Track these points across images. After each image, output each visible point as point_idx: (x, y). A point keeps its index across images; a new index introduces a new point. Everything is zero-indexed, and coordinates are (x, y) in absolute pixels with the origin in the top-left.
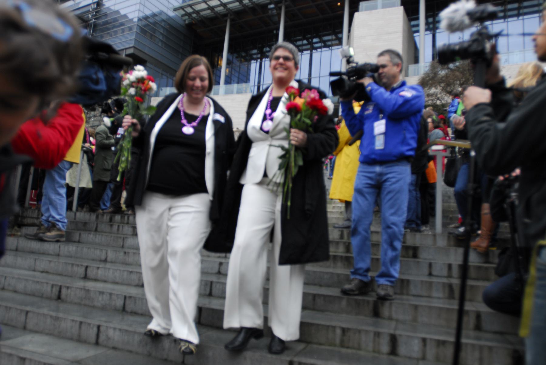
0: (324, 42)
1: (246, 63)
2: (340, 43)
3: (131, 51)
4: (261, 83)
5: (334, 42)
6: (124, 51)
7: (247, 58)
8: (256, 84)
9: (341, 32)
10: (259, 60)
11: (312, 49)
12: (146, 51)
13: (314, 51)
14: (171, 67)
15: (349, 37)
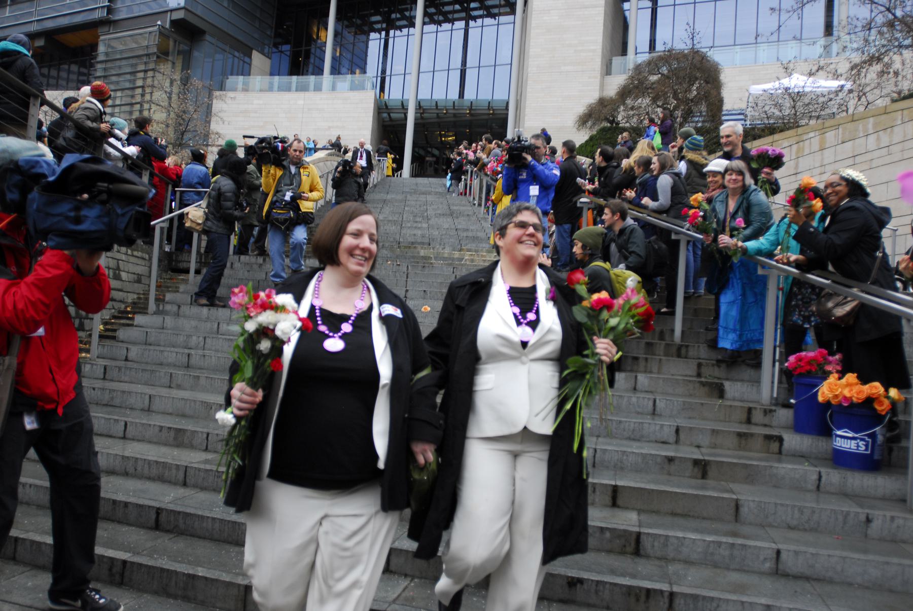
1: (363, 37)
2: (513, 12)
4: (388, 72)
5: (502, 10)
7: (366, 28)
10: (383, 33)
11: (469, 18)
12: (199, 11)
13: (472, 23)
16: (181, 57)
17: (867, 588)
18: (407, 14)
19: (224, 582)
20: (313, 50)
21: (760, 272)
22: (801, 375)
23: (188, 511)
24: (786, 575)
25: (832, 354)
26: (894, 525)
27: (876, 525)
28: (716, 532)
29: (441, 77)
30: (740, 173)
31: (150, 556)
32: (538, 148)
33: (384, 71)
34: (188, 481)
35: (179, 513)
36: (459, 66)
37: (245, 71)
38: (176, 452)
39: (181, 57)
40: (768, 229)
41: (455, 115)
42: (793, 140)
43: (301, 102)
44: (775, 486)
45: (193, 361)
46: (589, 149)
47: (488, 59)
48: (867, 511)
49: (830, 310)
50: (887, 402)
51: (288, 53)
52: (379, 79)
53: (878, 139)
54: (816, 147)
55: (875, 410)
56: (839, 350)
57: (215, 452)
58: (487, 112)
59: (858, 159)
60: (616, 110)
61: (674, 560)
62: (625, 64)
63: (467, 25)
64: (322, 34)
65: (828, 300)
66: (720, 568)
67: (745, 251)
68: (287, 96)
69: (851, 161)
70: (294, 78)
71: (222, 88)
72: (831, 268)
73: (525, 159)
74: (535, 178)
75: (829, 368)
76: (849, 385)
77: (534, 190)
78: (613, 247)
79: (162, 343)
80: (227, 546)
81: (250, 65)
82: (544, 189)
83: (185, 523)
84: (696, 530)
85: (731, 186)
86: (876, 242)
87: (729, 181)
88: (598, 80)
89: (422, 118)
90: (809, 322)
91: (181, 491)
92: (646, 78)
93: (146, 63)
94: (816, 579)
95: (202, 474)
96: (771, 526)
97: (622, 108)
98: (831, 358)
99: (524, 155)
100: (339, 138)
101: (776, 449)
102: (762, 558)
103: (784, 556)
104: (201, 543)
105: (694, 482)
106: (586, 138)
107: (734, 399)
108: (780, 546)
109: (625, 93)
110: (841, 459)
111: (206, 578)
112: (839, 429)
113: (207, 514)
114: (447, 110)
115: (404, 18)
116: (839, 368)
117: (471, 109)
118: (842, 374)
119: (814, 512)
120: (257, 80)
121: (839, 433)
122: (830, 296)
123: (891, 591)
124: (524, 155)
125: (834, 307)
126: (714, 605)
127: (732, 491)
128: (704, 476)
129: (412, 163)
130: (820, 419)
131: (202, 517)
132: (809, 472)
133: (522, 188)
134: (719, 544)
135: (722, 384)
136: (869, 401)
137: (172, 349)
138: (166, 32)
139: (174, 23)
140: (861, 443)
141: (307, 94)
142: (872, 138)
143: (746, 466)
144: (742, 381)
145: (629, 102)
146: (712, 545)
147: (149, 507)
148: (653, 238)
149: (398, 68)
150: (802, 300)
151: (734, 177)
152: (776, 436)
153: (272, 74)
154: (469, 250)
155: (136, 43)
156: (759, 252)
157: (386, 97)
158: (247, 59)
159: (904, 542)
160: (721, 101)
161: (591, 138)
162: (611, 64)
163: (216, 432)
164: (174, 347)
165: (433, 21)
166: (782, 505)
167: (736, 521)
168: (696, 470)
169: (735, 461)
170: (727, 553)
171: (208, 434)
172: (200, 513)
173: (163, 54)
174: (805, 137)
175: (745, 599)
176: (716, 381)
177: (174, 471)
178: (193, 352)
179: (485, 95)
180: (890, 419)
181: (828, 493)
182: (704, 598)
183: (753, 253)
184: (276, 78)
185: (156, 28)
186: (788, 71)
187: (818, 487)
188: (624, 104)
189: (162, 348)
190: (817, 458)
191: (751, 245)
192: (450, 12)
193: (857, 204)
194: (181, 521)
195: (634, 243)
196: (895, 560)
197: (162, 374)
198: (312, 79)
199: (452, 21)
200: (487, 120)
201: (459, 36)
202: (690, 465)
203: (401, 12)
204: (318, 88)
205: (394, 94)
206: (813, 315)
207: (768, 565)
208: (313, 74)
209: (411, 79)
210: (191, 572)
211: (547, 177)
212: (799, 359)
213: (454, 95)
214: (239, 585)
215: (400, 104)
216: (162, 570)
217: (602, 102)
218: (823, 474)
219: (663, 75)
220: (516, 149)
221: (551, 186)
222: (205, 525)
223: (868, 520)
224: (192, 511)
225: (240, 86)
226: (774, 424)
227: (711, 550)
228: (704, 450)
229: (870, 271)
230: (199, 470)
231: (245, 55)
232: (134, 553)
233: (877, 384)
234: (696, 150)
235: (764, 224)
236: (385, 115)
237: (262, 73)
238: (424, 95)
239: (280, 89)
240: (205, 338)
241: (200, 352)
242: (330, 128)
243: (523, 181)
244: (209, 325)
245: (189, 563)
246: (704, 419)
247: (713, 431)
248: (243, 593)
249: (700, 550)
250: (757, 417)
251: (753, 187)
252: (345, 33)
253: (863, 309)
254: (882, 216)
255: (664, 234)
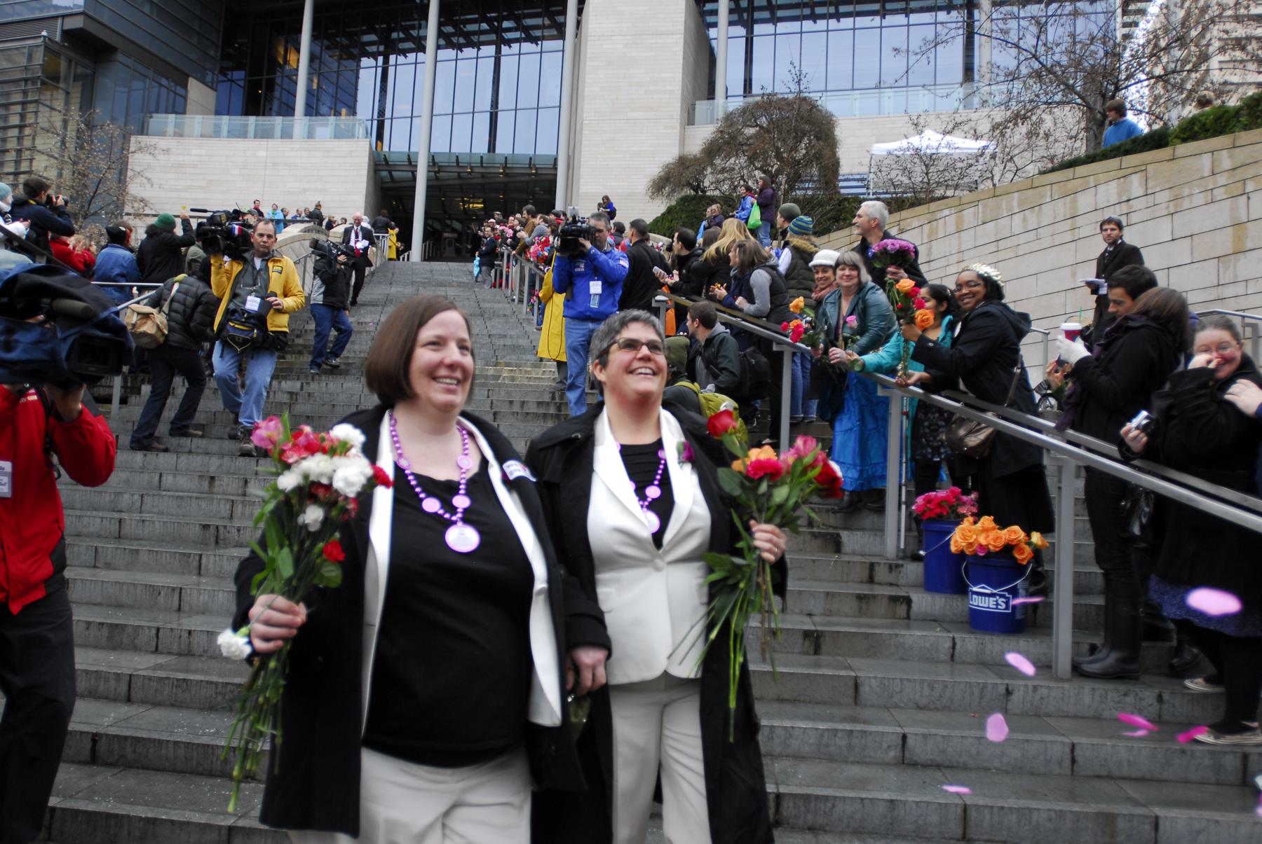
0: (526, 30)
2: (561, 35)
3: (77, 23)
4: (388, 114)
5: (547, 33)
6: (60, 20)
7: (355, 51)
8: (375, 116)
9: (564, 12)
10: (381, 59)
11: (500, 42)
12: (106, 18)
13: (505, 49)
14: (170, 59)
15: (579, 23)
16: (80, 84)
17: (1007, 772)
18: (414, 33)
19: (199, 824)
20: (278, 81)
21: (880, 392)
22: (930, 520)
23: (138, 734)
24: (914, 765)
25: (967, 492)
26: (1037, 697)
27: (1017, 697)
28: (831, 719)
29: (462, 123)
30: (855, 267)
31: (89, 798)
32: (600, 231)
33: (382, 112)
34: (133, 694)
35: (126, 738)
36: (488, 107)
37: (178, 107)
38: (112, 656)
39: (80, 84)
40: (890, 336)
41: (483, 175)
42: (924, 219)
43: (263, 154)
44: (902, 659)
45: (126, 529)
46: (667, 224)
47: (527, 99)
48: (1006, 681)
49: (962, 439)
50: (1028, 549)
51: (242, 83)
52: (375, 123)
53: (1025, 220)
54: (952, 229)
55: (1015, 559)
56: (974, 489)
57: (169, 653)
58: (528, 171)
59: (1002, 244)
60: (701, 172)
61: (781, 756)
62: (713, 111)
63: (498, 51)
64: (292, 57)
65: (960, 427)
66: (837, 761)
67: (864, 365)
68: (241, 144)
69: (993, 247)
70: (252, 120)
71: (142, 130)
72: (962, 386)
73: (584, 246)
74: (596, 271)
75: (963, 510)
76: (985, 530)
77: (596, 287)
78: (699, 360)
79: (78, 505)
80: (197, 779)
81: (185, 98)
82: (608, 284)
83: (134, 751)
84: (808, 718)
85: (845, 284)
86: (1013, 356)
87: (841, 278)
88: (677, 131)
89: (437, 178)
90: (939, 455)
91: (125, 710)
92: (740, 132)
93: (25, 93)
94: (948, 767)
95: (154, 684)
96: (896, 707)
97: (709, 170)
98: (965, 498)
99: (582, 240)
100: (318, 206)
101: (904, 614)
102: (885, 746)
103: (910, 741)
104: (160, 777)
105: (805, 658)
106: (663, 209)
107: (854, 554)
108: (907, 730)
109: (712, 150)
110: (980, 622)
111: (172, 822)
112: (975, 585)
113: (165, 737)
114: (471, 168)
115: (409, 38)
116: (975, 510)
117: (505, 167)
118: (977, 516)
119: (946, 687)
120: (196, 121)
121: (975, 589)
122: (962, 421)
123: (1032, 774)
124: (582, 240)
125: (966, 435)
126: (829, 805)
127: (850, 668)
128: (817, 651)
129: (425, 240)
130: (953, 573)
131: (160, 741)
132: (940, 638)
133: (579, 283)
134: (835, 731)
135: (838, 535)
136: (1008, 548)
137: (94, 513)
138: (56, 48)
139: (67, 34)
140: (1001, 601)
141: (271, 143)
142: (1017, 219)
143: (867, 635)
144: (864, 529)
145: (718, 161)
146: (826, 734)
147: (82, 733)
148: (749, 350)
149: (402, 108)
150: (929, 427)
151: (847, 272)
152: (903, 597)
153: (218, 112)
154: (507, 365)
155: (9, 60)
156: (879, 368)
157: (386, 149)
158: (180, 90)
159: (1049, 716)
160: (836, 164)
161: (669, 210)
162: (694, 110)
163: (169, 626)
164: (95, 510)
165: (450, 45)
166: (909, 680)
167: (856, 704)
168: (807, 643)
169: (853, 630)
170: (844, 743)
171: (158, 630)
172: (156, 736)
173: (51, 79)
174: (939, 215)
175: (864, 795)
176: (831, 531)
177: (112, 683)
178: (125, 516)
179: (524, 149)
180: (1033, 569)
181: (964, 663)
182: (817, 797)
183: (870, 369)
184: (225, 118)
185: (39, 41)
186: (918, 127)
187: (952, 656)
188: (712, 164)
189: (79, 513)
190: (951, 622)
191: (870, 358)
192: (474, 33)
193: (991, 308)
194: (129, 749)
195: (725, 357)
196: (1037, 737)
197: (83, 549)
198: (278, 121)
199: (477, 45)
200: (528, 182)
201: (487, 66)
202: (800, 638)
203: (406, 30)
204: (287, 134)
205: (397, 144)
206: (943, 445)
207: (892, 754)
208: (279, 114)
209: (421, 124)
210: (150, 815)
211: (612, 269)
212: (928, 501)
213: (481, 147)
214: (220, 827)
215: (405, 158)
216: (108, 816)
217: (683, 162)
218: (957, 641)
219: (761, 127)
220: (571, 233)
221: (618, 281)
222: (163, 752)
223: (1009, 692)
224: (145, 735)
225: (171, 129)
226: (902, 582)
227: (825, 740)
228: (817, 619)
229: (1006, 390)
230: (150, 678)
231: (177, 84)
232: (64, 796)
233: (1016, 528)
234: (803, 234)
235: (882, 329)
236: (384, 174)
237: (203, 114)
238: (440, 147)
239: (231, 134)
240: (142, 496)
241: (136, 516)
242: (305, 190)
243: (581, 275)
244: (146, 477)
245: (146, 804)
246: (816, 580)
247: (827, 594)
248: (225, 838)
249: (812, 741)
250: (882, 574)
251: (871, 284)
252: (326, 57)
253: (999, 437)
254: (1020, 325)
255: (763, 344)
